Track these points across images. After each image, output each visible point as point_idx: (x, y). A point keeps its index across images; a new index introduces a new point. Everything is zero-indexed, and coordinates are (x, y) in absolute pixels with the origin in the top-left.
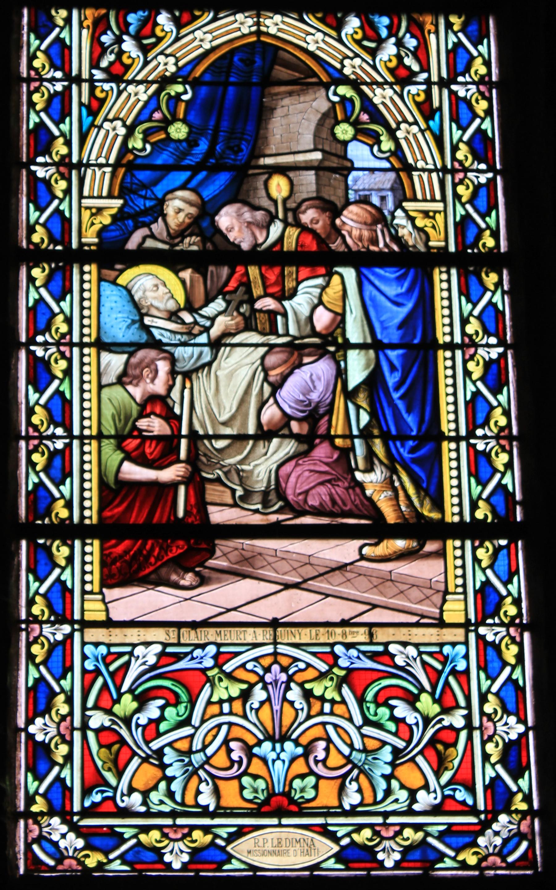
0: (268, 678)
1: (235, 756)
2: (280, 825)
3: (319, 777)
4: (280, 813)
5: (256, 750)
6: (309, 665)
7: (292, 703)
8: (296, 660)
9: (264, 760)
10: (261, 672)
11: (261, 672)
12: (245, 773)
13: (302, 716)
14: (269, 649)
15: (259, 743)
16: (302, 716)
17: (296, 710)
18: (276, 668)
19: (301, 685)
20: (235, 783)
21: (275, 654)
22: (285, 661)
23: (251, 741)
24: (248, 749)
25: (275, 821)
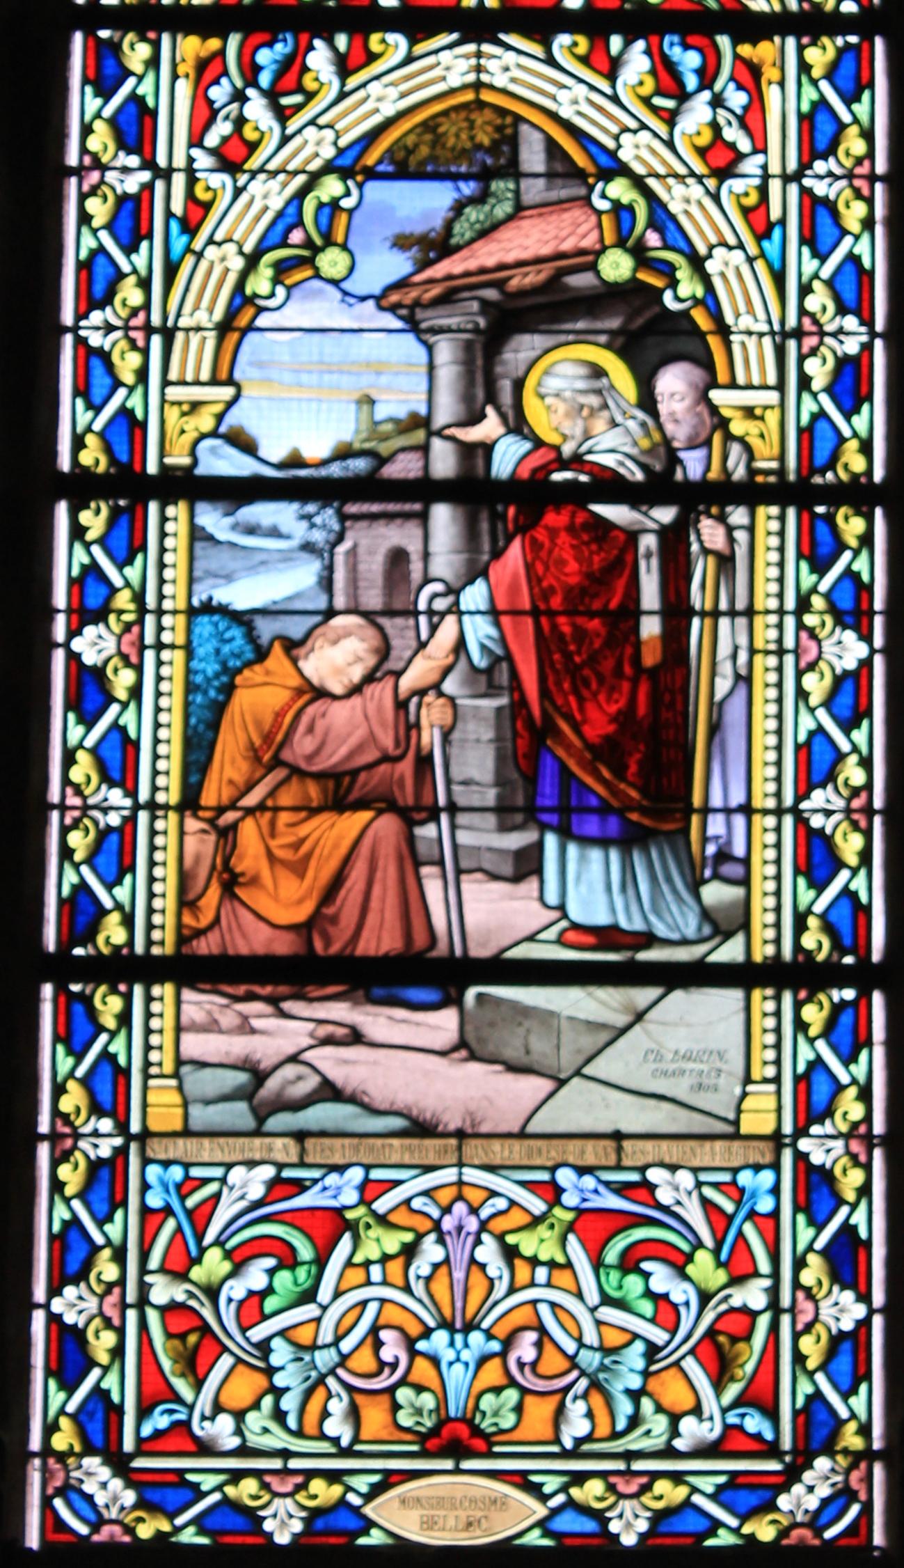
0: (448, 1223)
1: (387, 1354)
2: (457, 1471)
3: (524, 1391)
4: (457, 1450)
5: (421, 1345)
6: (513, 1203)
7: (483, 1267)
8: (494, 1194)
9: (435, 1361)
10: (435, 1213)
11: (435, 1213)
12: (403, 1382)
13: (501, 1288)
14: (449, 1175)
15: (427, 1333)
16: (501, 1288)
17: (491, 1281)
18: (460, 1208)
19: (500, 1238)
20: (384, 1400)
21: (460, 1183)
22: (474, 1196)
23: (414, 1329)
24: (410, 1343)
25: (448, 1464)
